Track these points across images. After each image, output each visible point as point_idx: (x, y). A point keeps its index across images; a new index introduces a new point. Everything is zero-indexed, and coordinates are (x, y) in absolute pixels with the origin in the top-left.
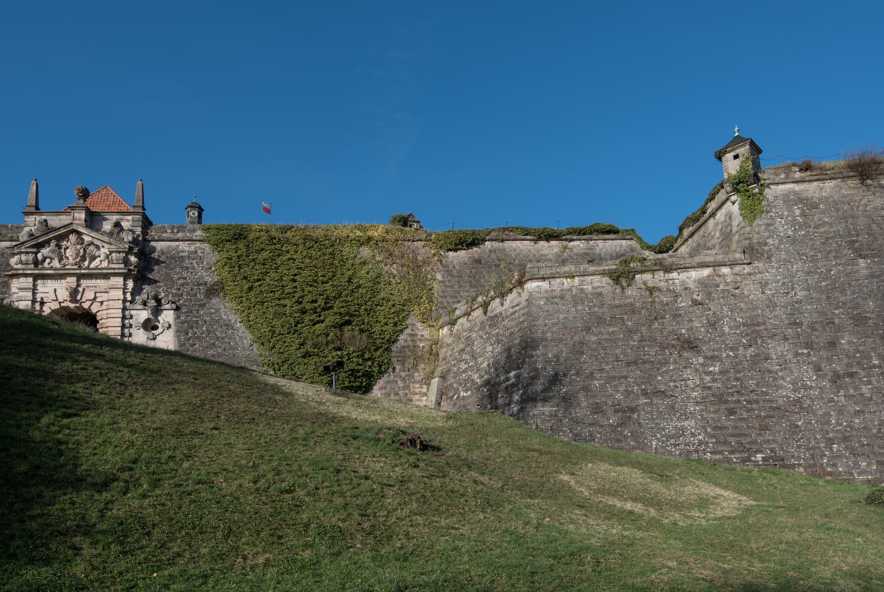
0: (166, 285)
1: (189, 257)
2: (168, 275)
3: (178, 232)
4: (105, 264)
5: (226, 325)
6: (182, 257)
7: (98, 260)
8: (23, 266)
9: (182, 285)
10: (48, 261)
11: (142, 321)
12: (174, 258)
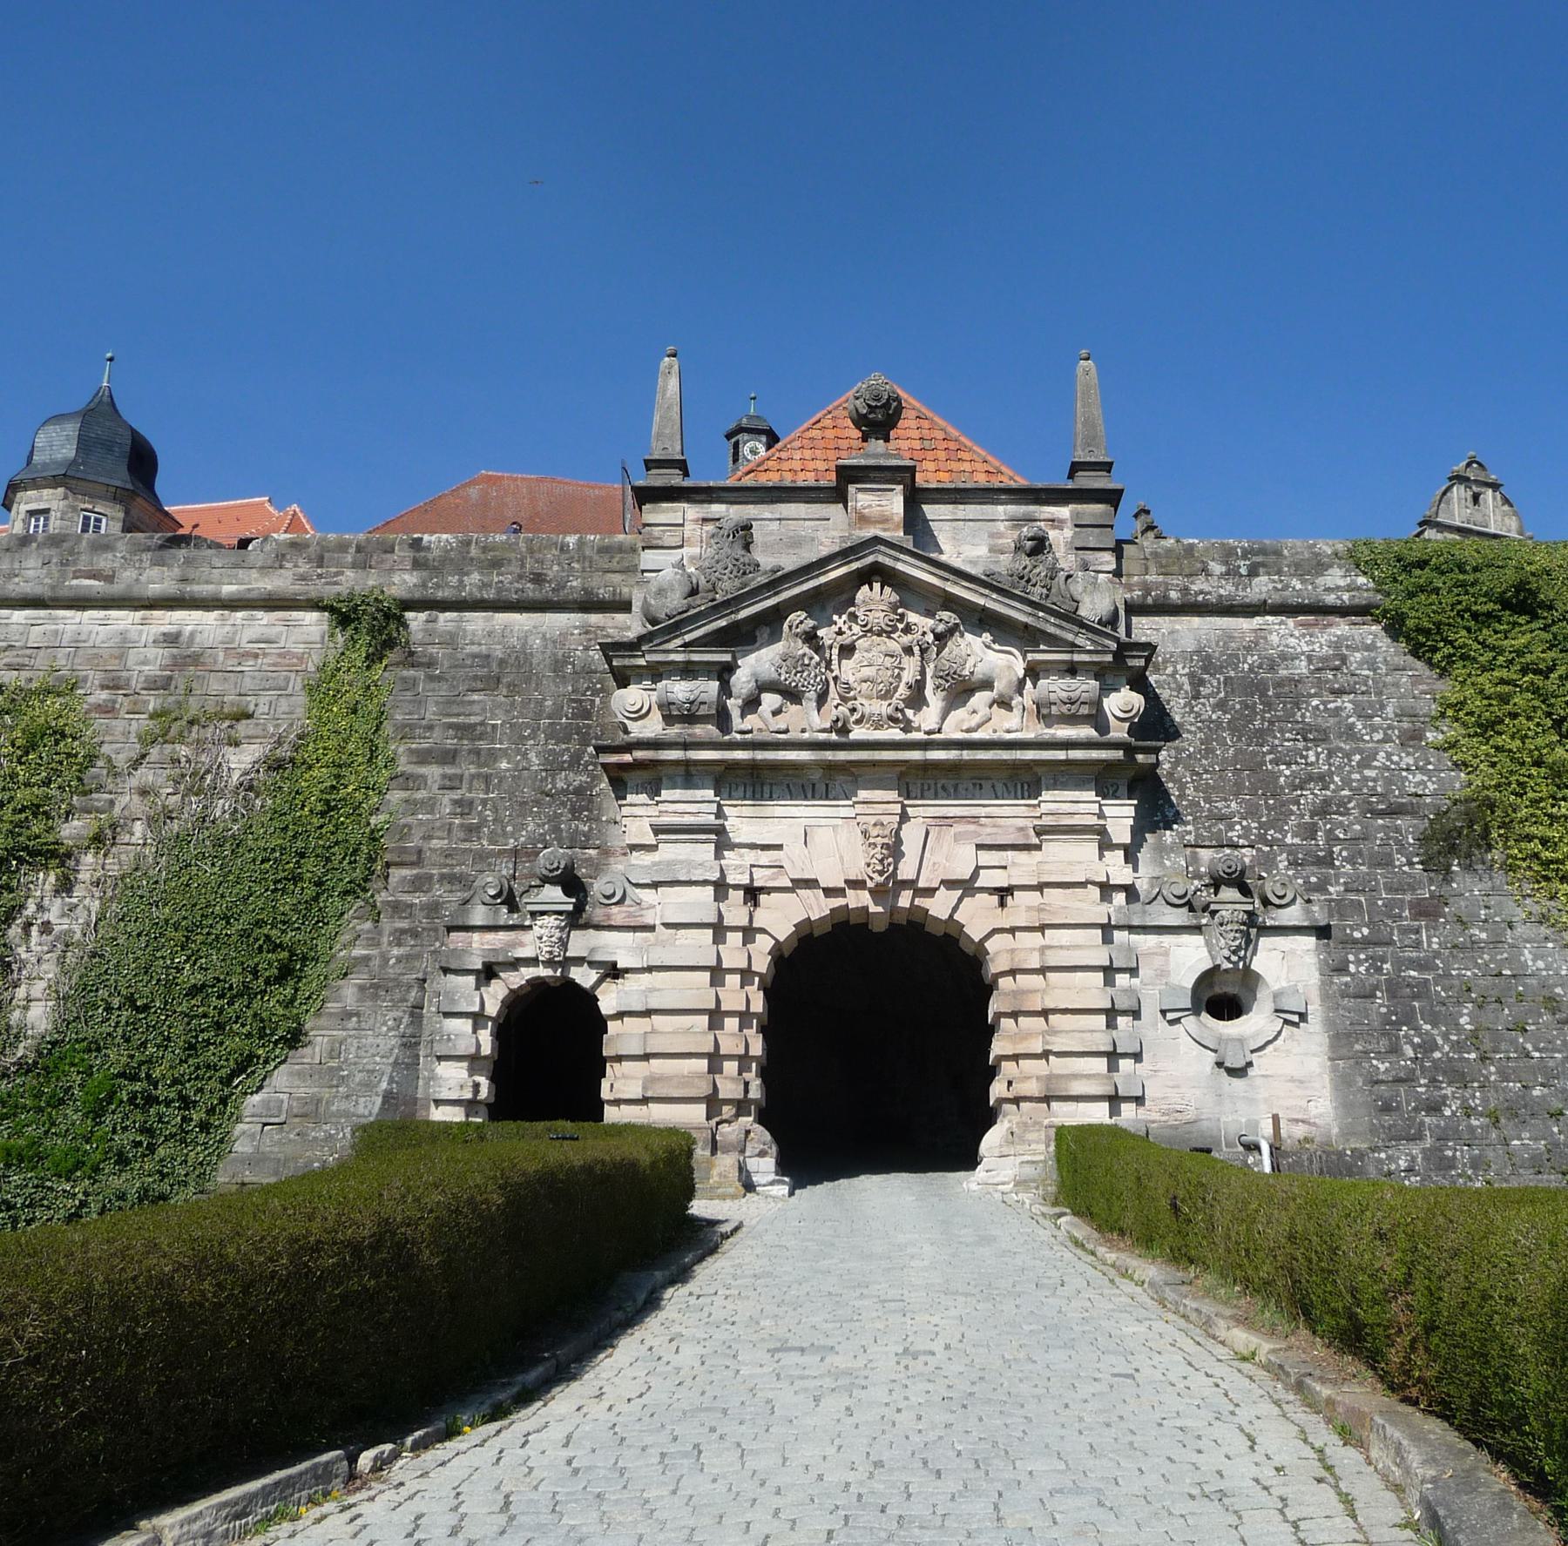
0: (1251, 812)
1: (1320, 683)
3: (1253, 572)
4: (1009, 724)
6: (1296, 682)
7: (980, 699)
8: (675, 731)
9: (1323, 810)
10: (770, 700)
11: (1189, 983)
12: (1261, 688)
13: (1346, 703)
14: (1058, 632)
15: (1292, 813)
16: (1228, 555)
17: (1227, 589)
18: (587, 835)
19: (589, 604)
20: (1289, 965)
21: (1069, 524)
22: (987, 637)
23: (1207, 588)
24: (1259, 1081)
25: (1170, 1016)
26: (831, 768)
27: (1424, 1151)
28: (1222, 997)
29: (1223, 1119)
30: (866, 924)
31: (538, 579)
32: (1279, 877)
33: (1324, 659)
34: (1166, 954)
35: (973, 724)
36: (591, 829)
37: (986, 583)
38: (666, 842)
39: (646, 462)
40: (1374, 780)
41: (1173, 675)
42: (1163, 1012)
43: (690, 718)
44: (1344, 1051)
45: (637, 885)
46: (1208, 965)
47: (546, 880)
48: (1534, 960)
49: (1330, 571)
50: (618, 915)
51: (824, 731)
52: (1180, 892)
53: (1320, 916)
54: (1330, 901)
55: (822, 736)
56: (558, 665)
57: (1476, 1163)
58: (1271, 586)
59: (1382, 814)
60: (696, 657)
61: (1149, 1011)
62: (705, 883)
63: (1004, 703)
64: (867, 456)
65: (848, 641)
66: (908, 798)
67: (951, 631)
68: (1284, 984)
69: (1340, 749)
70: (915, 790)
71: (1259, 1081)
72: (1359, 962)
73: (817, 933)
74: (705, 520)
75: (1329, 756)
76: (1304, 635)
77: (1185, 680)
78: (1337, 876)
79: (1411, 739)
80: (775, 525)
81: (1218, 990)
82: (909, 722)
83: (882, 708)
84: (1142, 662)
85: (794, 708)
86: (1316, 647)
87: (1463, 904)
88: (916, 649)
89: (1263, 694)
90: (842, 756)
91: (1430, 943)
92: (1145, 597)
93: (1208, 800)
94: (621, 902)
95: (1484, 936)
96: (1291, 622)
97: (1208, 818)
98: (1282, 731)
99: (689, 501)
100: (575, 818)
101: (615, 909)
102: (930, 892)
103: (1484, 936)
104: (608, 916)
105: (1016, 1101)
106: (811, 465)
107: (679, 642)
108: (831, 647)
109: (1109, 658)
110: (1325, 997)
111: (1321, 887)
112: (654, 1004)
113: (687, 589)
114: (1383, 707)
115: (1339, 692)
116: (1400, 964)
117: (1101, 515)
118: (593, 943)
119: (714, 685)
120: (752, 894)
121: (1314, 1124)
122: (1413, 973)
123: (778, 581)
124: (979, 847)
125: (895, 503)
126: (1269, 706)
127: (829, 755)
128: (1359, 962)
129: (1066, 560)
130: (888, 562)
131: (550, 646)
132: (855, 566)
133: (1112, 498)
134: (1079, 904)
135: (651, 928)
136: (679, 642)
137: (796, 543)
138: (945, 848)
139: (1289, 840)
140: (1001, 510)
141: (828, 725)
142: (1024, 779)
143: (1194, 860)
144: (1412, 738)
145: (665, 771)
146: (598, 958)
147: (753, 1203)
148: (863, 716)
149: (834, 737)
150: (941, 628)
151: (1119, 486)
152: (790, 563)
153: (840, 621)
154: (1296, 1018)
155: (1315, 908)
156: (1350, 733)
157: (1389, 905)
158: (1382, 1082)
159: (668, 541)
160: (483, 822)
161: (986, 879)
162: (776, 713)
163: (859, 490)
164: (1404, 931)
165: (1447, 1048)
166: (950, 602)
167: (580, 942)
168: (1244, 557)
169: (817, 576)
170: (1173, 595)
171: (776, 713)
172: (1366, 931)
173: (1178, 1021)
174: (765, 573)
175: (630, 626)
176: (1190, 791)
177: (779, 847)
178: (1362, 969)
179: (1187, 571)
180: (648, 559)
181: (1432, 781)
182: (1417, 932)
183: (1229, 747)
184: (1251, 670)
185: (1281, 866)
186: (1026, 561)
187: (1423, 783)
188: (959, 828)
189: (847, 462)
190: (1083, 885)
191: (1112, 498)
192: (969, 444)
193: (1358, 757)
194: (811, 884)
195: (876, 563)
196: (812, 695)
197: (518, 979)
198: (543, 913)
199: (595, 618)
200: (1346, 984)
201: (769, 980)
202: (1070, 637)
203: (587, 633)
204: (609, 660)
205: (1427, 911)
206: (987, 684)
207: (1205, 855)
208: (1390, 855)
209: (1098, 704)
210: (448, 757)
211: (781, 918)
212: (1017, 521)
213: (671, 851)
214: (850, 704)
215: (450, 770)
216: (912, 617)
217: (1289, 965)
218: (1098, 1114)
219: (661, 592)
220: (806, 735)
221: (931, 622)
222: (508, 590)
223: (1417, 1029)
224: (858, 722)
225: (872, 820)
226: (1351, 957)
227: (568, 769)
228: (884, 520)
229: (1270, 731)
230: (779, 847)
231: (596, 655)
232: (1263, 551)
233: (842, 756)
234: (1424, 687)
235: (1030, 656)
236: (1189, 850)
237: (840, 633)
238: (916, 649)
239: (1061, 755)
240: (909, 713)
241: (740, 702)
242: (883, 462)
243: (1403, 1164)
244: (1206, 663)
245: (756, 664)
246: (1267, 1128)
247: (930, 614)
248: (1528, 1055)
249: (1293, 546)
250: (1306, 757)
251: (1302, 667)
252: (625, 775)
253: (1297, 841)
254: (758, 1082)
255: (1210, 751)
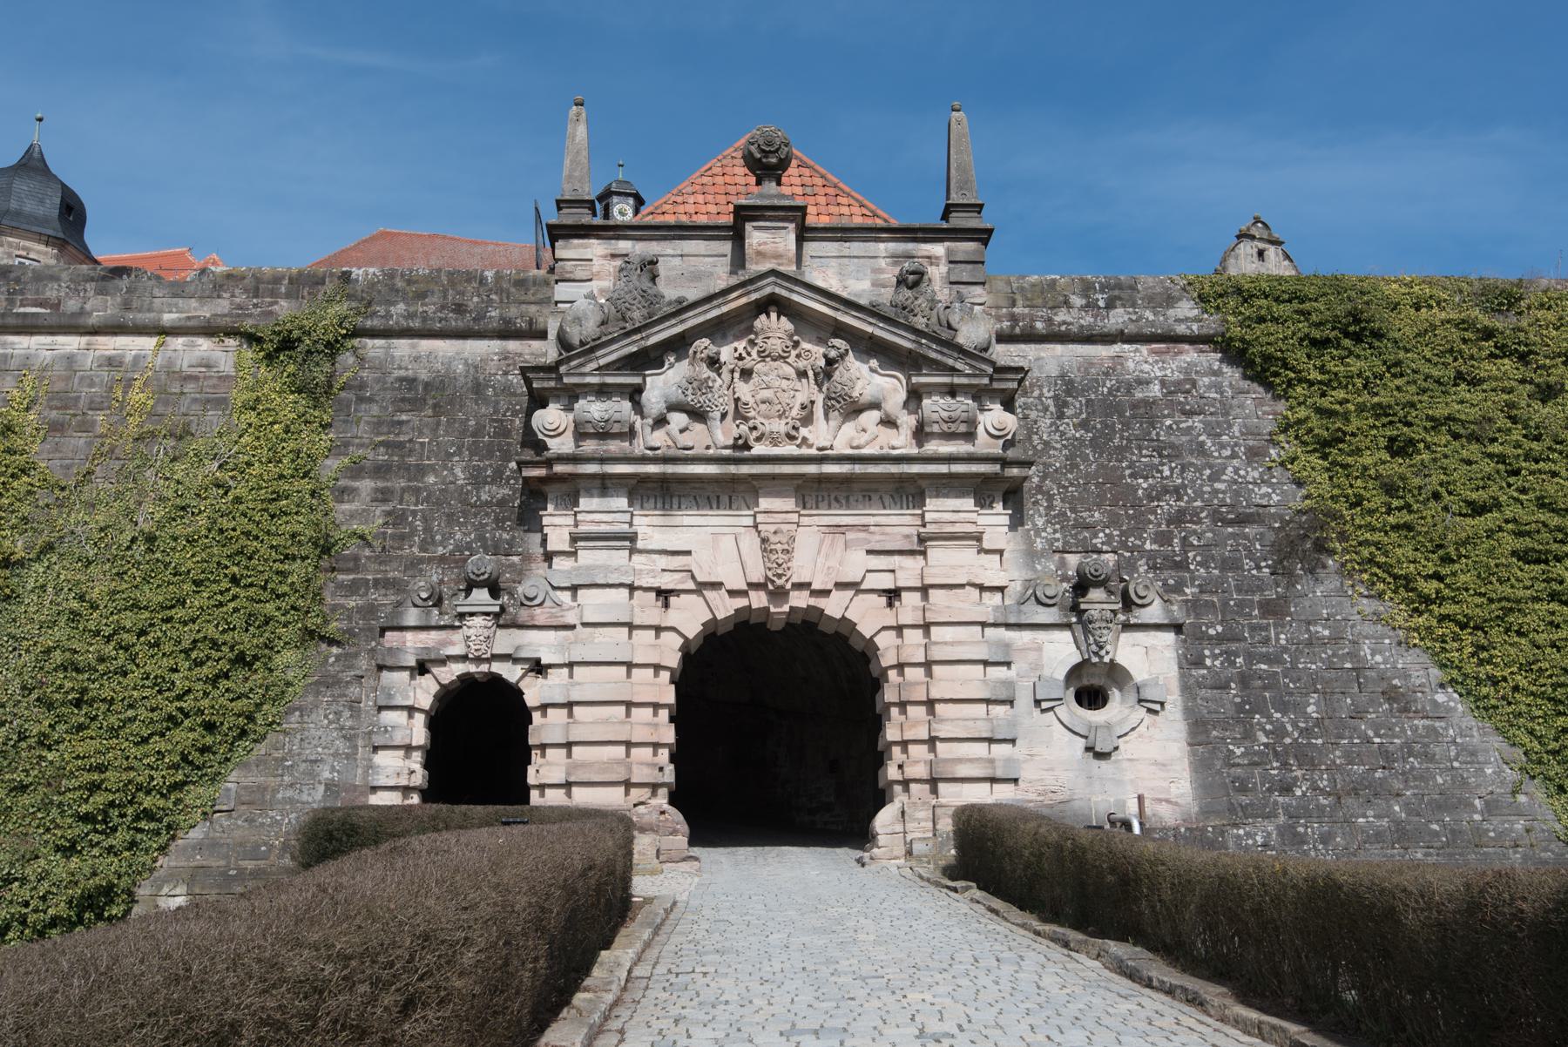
0: (1114, 521)
2: (1114, 478)
3: (1110, 305)
5: (1391, 695)
6: (1149, 404)
9: (1178, 518)
11: (1061, 674)
12: (1117, 409)
13: (1197, 422)
14: (939, 357)
15: (1150, 522)
16: (1087, 289)
17: (1087, 320)
18: (511, 543)
19: (506, 332)
20: (1147, 656)
21: (943, 261)
22: (874, 363)
23: (1069, 319)
24: (1125, 764)
25: (1045, 705)
26: (735, 480)
27: (1278, 827)
28: (1090, 688)
29: (1094, 799)
30: (763, 624)
31: (460, 309)
32: (1141, 580)
33: (1178, 383)
34: (1039, 649)
35: (862, 441)
36: (513, 537)
37: (872, 311)
38: (585, 548)
39: (558, 202)
40: (1223, 492)
41: (1039, 398)
42: (1038, 702)
43: (604, 435)
44: (1202, 738)
45: (554, 588)
46: (1077, 659)
47: (471, 586)
48: (1373, 655)
49: (1180, 304)
50: (541, 616)
51: (726, 447)
52: (1050, 592)
53: (1177, 612)
54: (1187, 601)
55: (727, 452)
56: (478, 388)
57: (1326, 839)
58: (1126, 317)
59: (1231, 523)
60: (610, 380)
61: (1024, 700)
62: (621, 585)
63: (889, 422)
64: (761, 196)
65: (748, 366)
66: (804, 508)
67: (842, 356)
68: (1146, 677)
69: (1192, 464)
70: (810, 501)
71: (1125, 764)
72: (1215, 657)
73: (720, 631)
74: (613, 256)
75: (1183, 471)
76: (1157, 362)
77: (1050, 402)
78: (1193, 579)
79: (1254, 455)
80: (677, 261)
81: (1085, 682)
82: (805, 439)
83: (780, 426)
84: (1015, 385)
85: (698, 427)
86: (1168, 372)
87: (1307, 604)
88: (810, 373)
89: (1121, 415)
90: (745, 469)
91: (1278, 639)
92: (1013, 327)
93: (1073, 510)
94: (541, 604)
95: (1326, 633)
96: (1144, 349)
97: (1074, 527)
98: (1140, 448)
99: (598, 237)
100: (499, 528)
101: (538, 611)
102: (825, 593)
103: (1326, 633)
104: (532, 617)
105: (905, 783)
106: (703, 209)
107: (594, 365)
108: (732, 371)
109: (986, 381)
110: (1187, 689)
111: (1178, 588)
112: (575, 697)
113: (599, 318)
114: (1230, 426)
115: (1190, 414)
116: (1250, 657)
117: (975, 252)
118: (517, 643)
119: (627, 405)
120: (664, 595)
121: (1176, 804)
122: (1264, 667)
123: (682, 308)
124: (869, 552)
125: (786, 239)
126: (1127, 425)
127: (732, 469)
128: (1215, 657)
129: (943, 293)
130: (784, 293)
131: (472, 371)
132: (754, 296)
133: (983, 236)
134: (961, 605)
135: (573, 627)
136: (594, 365)
137: (697, 277)
138: (838, 555)
139: (1148, 546)
140: (882, 248)
141: (731, 442)
142: (909, 490)
143: (1063, 564)
144: (1256, 454)
145: (582, 484)
146: (523, 654)
147: (687, 881)
148: (763, 434)
149: (738, 454)
150: (833, 354)
151: (989, 226)
152: (692, 295)
153: (741, 345)
154: (1157, 707)
155: (1175, 608)
156: (1201, 450)
157: (1241, 604)
158: (1238, 765)
159: (579, 274)
160: (413, 532)
161: (873, 581)
162: (682, 431)
163: (755, 228)
164: (1253, 628)
165: (1296, 735)
166: (840, 330)
167: (505, 641)
168: (1102, 291)
169: (719, 306)
170: (1039, 325)
171: (682, 431)
172: (1220, 629)
173: (1052, 709)
174: (670, 303)
175: (546, 351)
176: (1057, 502)
177: (688, 553)
178: (1217, 663)
179: (1051, 304)
180: (562, 291)
181: (1275, 495)
182: (1266, 628)
183: (1091, 463)
184: (1110, 393)
185: (1141, 570)
186: (908, 293)
187: (1269, 495)
188: (851, 535)
189: (743, 202)
190: (962, 586)
191: (983, 236)
192: (848, 190)
193: (1208, 472)
194: (716, 586)
195: (773, 294)
196: (717, 415)
197: (450, 673)
198: (472, 614)
199: (513, 345)
200: (1203, 676)
201: (678, 675)
202: (950, 362)
203: (506, 358)
204: (528, 382)
205: (1273, 609)
206: (876, 406)
207: (1073, 560)
208: (1240, 559)
209: (972, 423)
210: (380, 471)
211: (690, 617)
212: (896, 258)
213: (587, 557)
214: (751, 423)
215: (380, 484)
216: (805, 345)
217: (1147, 656)
218: (979, 794)
219: (578, 320)
220: (711, 451)
221: (822, 350)
222: (432, 319)
223: (1269, 717)
224: (758, 439)
225: (772, 528)
226: (1207, 652)
227: (491, 483)
228: (778, 256)
229: (1128, 448)
230: (688, 553)
231: (515, 379)
232: (1119, 286)
233: (745, 469)
234: (1266, 408)
235: (914, 380)
236: (1057, 556)
237: (740, 358)
238: (810, 373)
239: (943, 469)
240: (804, 432)
241: (650, 421)
242: (776, 202)
243: (1259, 839)
244: (1068, 387)
245: (661, 385)
246: (1132, 807)
247: (821, 341)
248: (1369, 741)
249: (1147, 282)
250: (1161, 472)
251: (1155, 390)
252: (546, 488)
253: (1155, 547)
254: (672, 767)
255: (1075, 466)
